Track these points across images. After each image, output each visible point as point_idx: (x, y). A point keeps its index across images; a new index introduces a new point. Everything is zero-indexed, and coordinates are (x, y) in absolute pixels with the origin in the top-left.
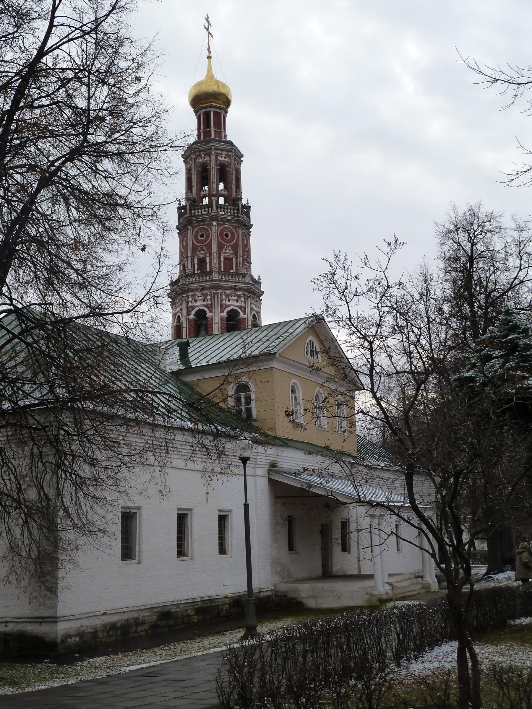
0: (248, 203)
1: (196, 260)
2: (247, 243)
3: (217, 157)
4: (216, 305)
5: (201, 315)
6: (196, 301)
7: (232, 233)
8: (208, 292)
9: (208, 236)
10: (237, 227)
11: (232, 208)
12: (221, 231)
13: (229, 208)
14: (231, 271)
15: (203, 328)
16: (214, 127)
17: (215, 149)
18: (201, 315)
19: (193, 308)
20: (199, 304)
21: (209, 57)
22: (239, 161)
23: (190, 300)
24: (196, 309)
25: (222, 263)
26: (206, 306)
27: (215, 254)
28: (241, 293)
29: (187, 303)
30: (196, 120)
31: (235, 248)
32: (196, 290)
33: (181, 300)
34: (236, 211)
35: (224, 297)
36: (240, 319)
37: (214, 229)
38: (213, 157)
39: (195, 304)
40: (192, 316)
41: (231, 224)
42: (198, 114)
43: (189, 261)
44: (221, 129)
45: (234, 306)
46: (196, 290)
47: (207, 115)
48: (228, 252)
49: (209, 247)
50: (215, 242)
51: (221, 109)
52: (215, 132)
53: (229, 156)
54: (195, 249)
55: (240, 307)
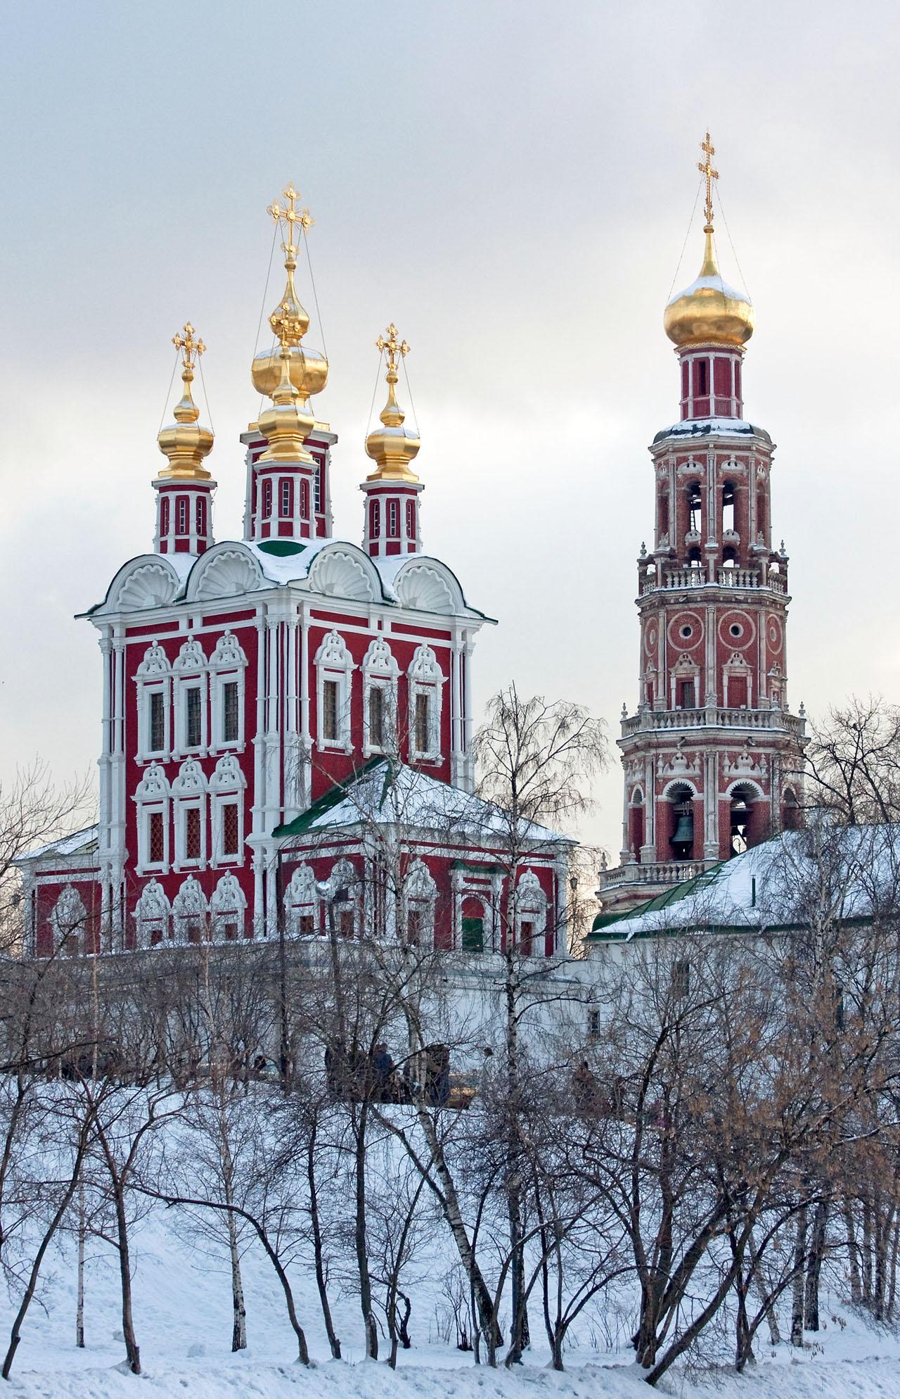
0: (782, 551)
1: (673, 681)
2: (779, 638)
3: (719, 464)
4: (710, 777)
5: (682, 794)
6: (672, 767)
7: (747, 625)
8: (696, 749)
9: (698, 633)
10: (756, 613)
11: (748, 572)
12: (724, 621)
13: (742, 572)
14: (743, 707)
15: (684, 820)
16: (716, 393)
17: (716, 447)
18: (682, 794)
19: (666, 780)
20: (679, 774)
21: (709, 230)
22: (767, 460)
23: (660, 763)
24: (670, 784)
25: (725, 690)
26: (691, 779)
27: (711, 672)
28: (761, 750)
29: (655, 770)
30: (679, 370)
31: (751, 657)
32: (673, 744)
33: (643, 760)
34: (755, 580)
35: (727, 762)
36: (757, 803)
37: (711, 617)
38: (711, 465)
39: (670, 773)
40: (664, 797)
41: (745, 606)
42: (685, 359)
43: (661, 681)
44: (729, 395)
45: (747, 777)
46: (673, 744)
47: (702, 365)
48: (738, 666)
49: (700, 657)
50: (710, 646)
51: (731, 351)
52: (717, 402)
53: (745, 460)
54: (672, 659)
55: (758, 781)
